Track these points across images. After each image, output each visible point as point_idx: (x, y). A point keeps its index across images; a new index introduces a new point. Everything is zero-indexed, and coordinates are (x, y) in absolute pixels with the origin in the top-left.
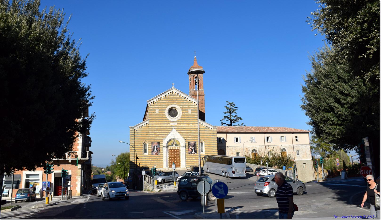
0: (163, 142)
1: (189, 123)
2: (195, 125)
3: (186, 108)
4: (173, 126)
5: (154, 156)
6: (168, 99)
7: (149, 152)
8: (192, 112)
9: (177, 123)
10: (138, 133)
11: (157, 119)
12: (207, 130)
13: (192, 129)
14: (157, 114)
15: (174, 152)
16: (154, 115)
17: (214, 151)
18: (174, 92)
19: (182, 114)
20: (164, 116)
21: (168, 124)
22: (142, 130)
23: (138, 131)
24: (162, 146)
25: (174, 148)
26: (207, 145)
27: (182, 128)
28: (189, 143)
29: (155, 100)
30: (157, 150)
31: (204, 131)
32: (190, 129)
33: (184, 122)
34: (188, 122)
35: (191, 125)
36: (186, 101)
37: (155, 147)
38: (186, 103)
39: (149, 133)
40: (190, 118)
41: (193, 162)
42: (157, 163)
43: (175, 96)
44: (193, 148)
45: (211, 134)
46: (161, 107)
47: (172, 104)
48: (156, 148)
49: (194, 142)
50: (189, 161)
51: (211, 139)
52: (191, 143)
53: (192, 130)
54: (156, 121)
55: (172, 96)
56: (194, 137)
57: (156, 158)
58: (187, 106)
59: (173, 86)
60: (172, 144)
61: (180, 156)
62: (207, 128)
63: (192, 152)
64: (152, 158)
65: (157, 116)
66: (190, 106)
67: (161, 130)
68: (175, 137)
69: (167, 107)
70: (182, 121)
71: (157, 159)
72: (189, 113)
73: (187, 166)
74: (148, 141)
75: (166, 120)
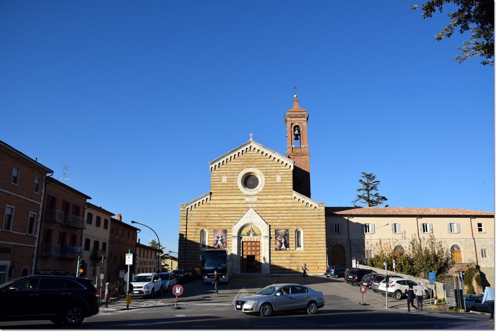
0: (232, 229)
1: (277, 198)
3: (272, 174)
4: (250, 203)
8: (282, 180)
9: (256, 198)
10: (192, 214)
11: (223, 191)
12: (309, 210)
13: (281, 209)
15: (252, 246)
17: (319, 245)
18: (252, 148)
19: (266, 183)
20: (235, 187)
21: (241, 200)
22: (199, 209)
23: (193, 211)
24: (230, 236)
25: (251, 239)
26: (308, 235)
27: (264, 206)
28: (276, 231)
29: (221, 161)
31: (302, 212)
33: (268, 196)
34: (275, 196)
35: (281, 201)
36: (271, 161)
38: (272, 165)
39: (209, 214)
40: (279, 189)
43: (254, 155)
44: (284, 240)
45: (315, 216)
46: (230, 173)
47: (248, 167)
48: (220, 239)
49: (285, 230)
51: (315, 225)
52: (279, 231)
53: (282, 210)
54: (222, 194)
55: (250, 155)
56: (285, 221)
58: (274, 171)
59: (251, 138)
60: (247, 233)
61: (261, 253)
62: (308, 207)
63: (281, 246)
65: (224, 187)
66: (278, 169)
67: (230, 209)
68: (252, 221)
69: (240, 173)
70: (265, 195)
73: (272, 271)
75: (238, 192)
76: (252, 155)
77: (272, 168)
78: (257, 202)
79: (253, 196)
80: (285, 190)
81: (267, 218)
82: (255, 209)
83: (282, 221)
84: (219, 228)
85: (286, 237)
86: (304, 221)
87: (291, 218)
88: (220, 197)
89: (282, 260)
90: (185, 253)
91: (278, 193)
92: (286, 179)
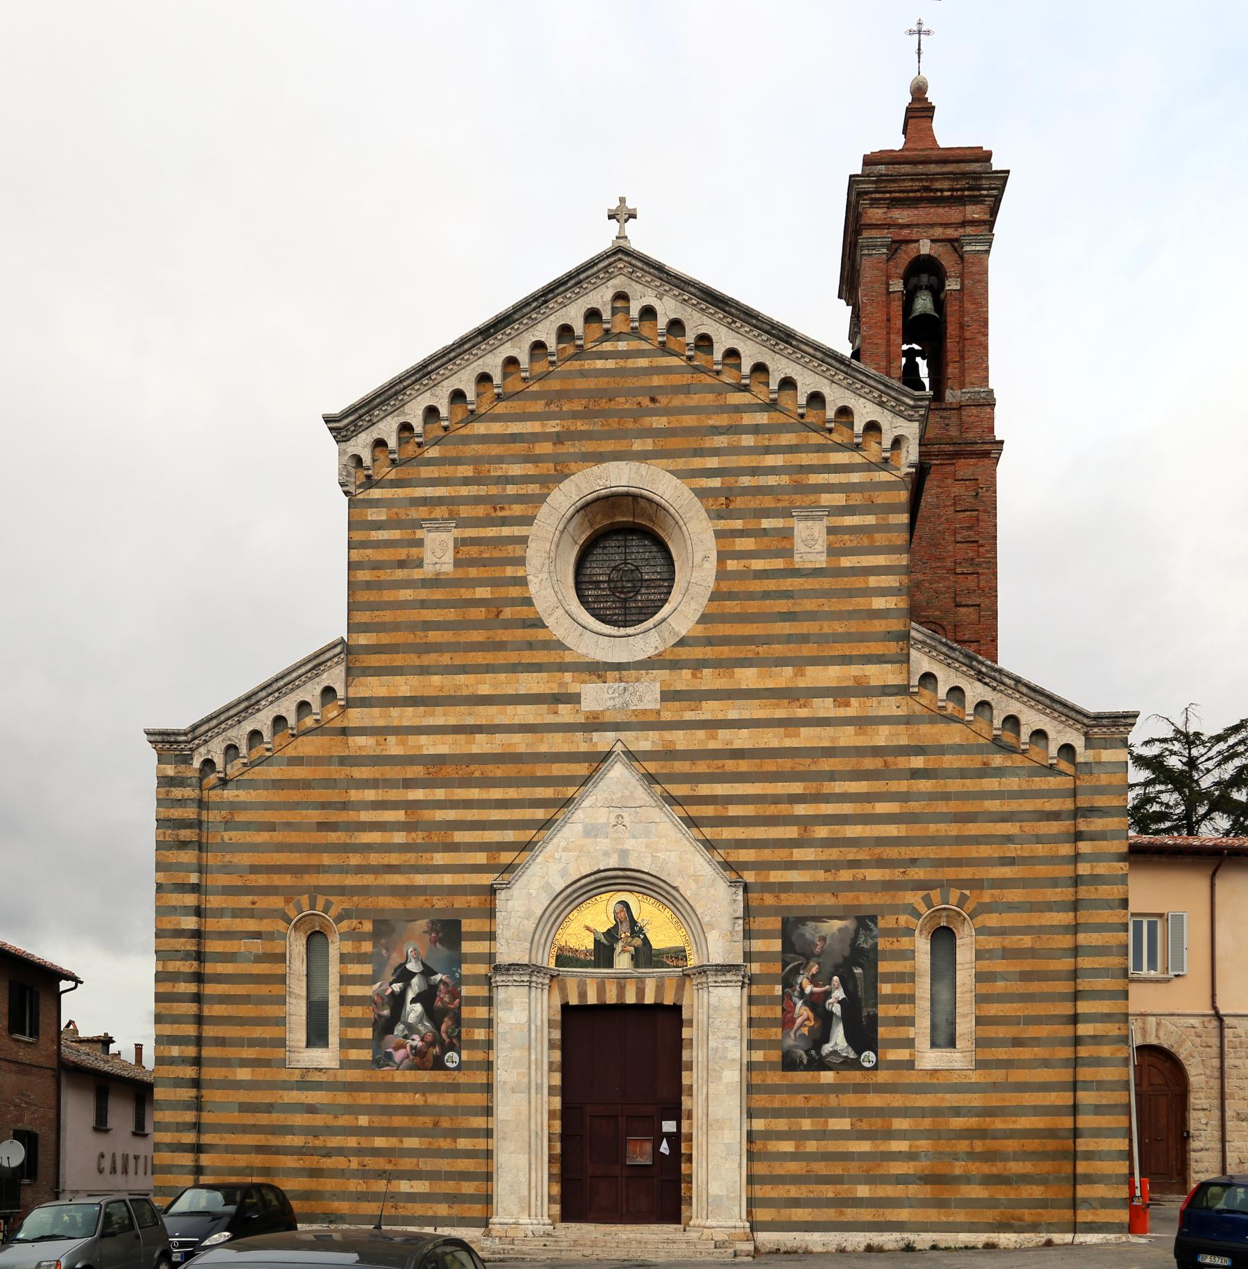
1: (802, 683)
2: (872, 713)
3: (768, 502)
4: (617, 727)
5: (400, 1077)
6: (563, 395)
7: (353, 1033)
8: (833, 552)
9: (657, 688)
10: (234, 806)
11: (434, 636)
13: (826, 765)
14: (435, 582)
16: (406, 594)
19: (722, 575)
20: (513, 602)
22: (273, 772)
26: (1007, 954)
27: (712, 745)
28: (790, 928)
30: (432, 1013)
31: (970, 785)
32: (804, 764)
33: (738, 672)
34: (788, 671)
35: (824, 707)
37: (415, 981)
38: (764, 440)
39: (345, 806)
40: (813, 616)
41: (837, 1169)
42: (426, 1164)
43: (643, 362)
44: (839, 994)
46: (477, 500)
47: (600, 458)
48: (416, 985)
50: (788, 1146)
52: (809, 930)
53: (833, 776)
55: (610, 364)
56: (851, 854)
57: (418, 1099)
58: (785, 480)
62: (1010, 750)
63: (827, 1040)
64: (382, 1099)
65: (437, 604)
66: (812, 469)
69: (542, 499)
70: (717, 664)
71: (425, 1121)
72: (797, 558)
73: (762, 1215)
74: (332, 899)
76: (631, 363)
77: (771, 460)
78: (658, 712)
79: (633, 673)
80: (854, 626)
81: (727, 833)
82: (652, 767)
83: (833, 854)
84: (407, 911)
85: (858, 971)
86: (985, 851)
87: (892, 830)
88: (414, 680)
89: (823, 1135)
90: (196, 1083)
91: (807, 650)
92: (866, 542)
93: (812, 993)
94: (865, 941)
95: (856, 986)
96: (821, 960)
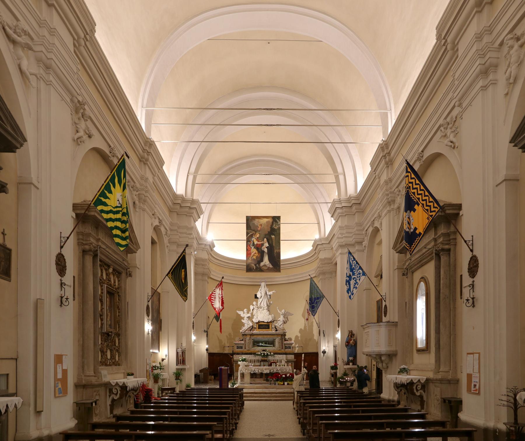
44: (267, 245)
63: (262, 260)
85: (273, 236)
93: (257, 244)
94: (276, 226)
95: (272, 242)
96: (260, 232)
